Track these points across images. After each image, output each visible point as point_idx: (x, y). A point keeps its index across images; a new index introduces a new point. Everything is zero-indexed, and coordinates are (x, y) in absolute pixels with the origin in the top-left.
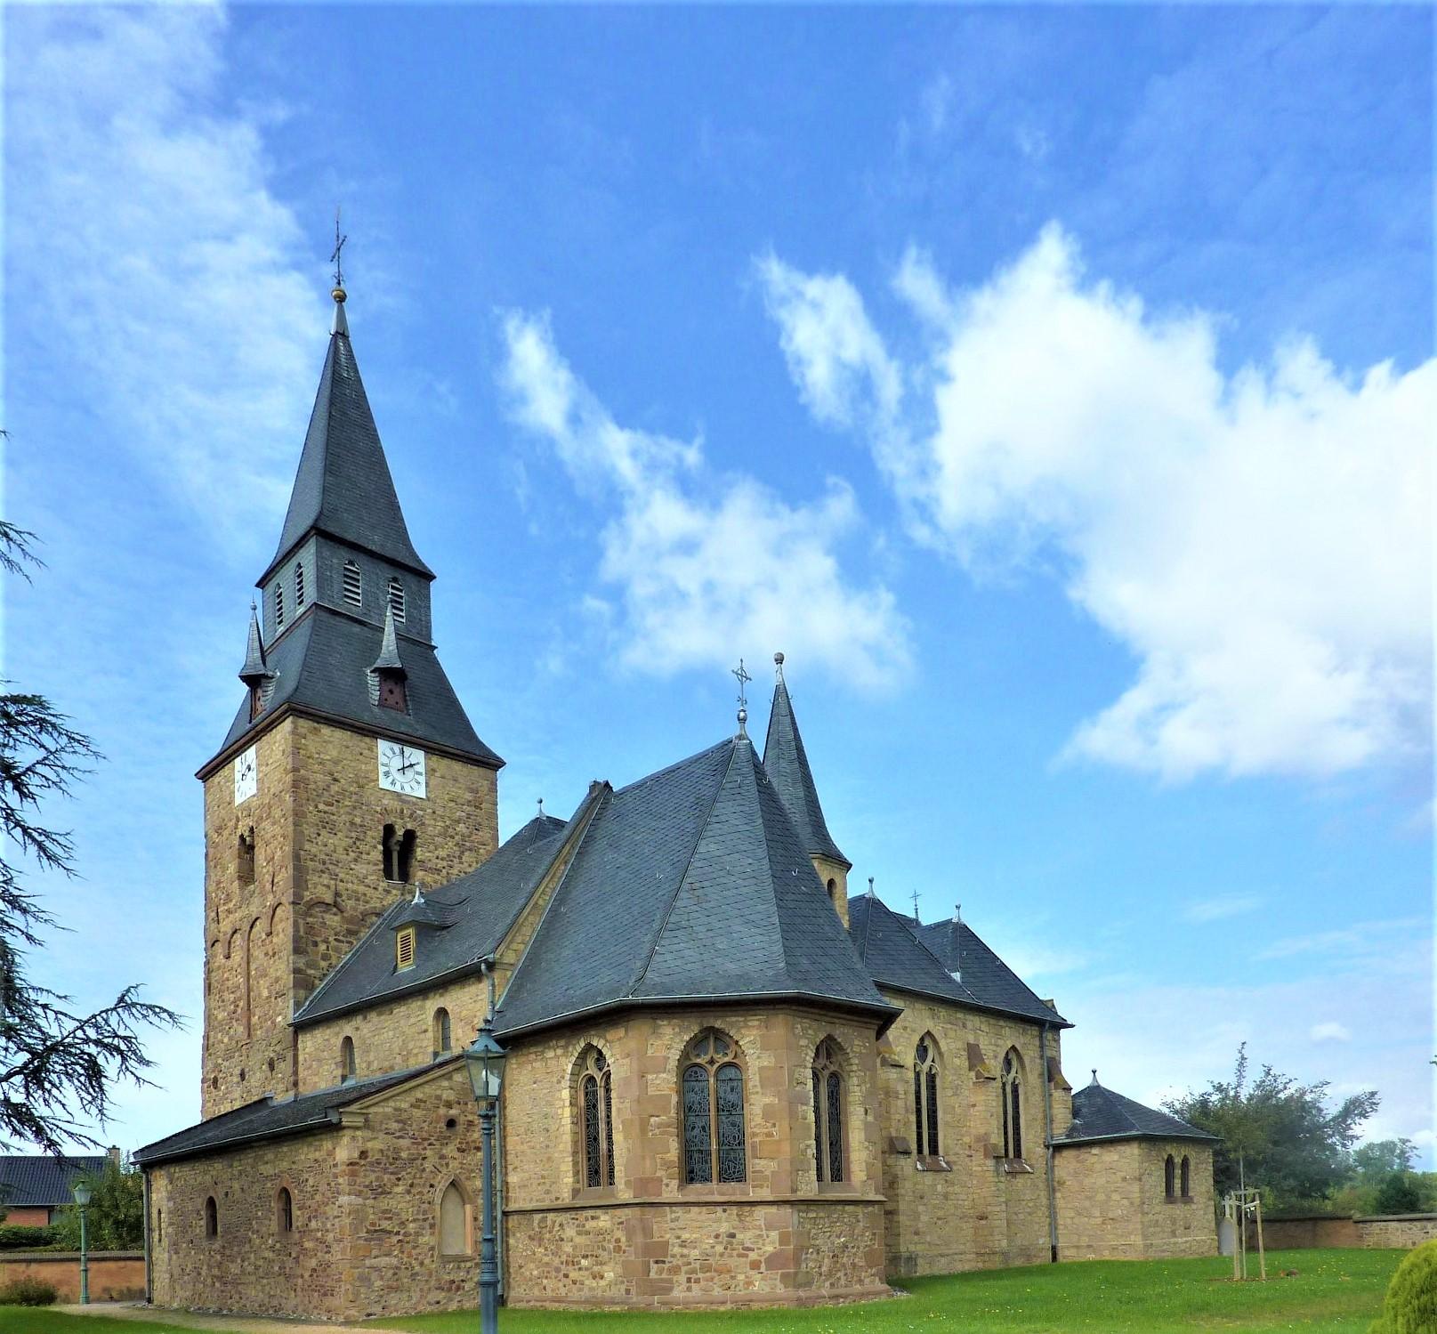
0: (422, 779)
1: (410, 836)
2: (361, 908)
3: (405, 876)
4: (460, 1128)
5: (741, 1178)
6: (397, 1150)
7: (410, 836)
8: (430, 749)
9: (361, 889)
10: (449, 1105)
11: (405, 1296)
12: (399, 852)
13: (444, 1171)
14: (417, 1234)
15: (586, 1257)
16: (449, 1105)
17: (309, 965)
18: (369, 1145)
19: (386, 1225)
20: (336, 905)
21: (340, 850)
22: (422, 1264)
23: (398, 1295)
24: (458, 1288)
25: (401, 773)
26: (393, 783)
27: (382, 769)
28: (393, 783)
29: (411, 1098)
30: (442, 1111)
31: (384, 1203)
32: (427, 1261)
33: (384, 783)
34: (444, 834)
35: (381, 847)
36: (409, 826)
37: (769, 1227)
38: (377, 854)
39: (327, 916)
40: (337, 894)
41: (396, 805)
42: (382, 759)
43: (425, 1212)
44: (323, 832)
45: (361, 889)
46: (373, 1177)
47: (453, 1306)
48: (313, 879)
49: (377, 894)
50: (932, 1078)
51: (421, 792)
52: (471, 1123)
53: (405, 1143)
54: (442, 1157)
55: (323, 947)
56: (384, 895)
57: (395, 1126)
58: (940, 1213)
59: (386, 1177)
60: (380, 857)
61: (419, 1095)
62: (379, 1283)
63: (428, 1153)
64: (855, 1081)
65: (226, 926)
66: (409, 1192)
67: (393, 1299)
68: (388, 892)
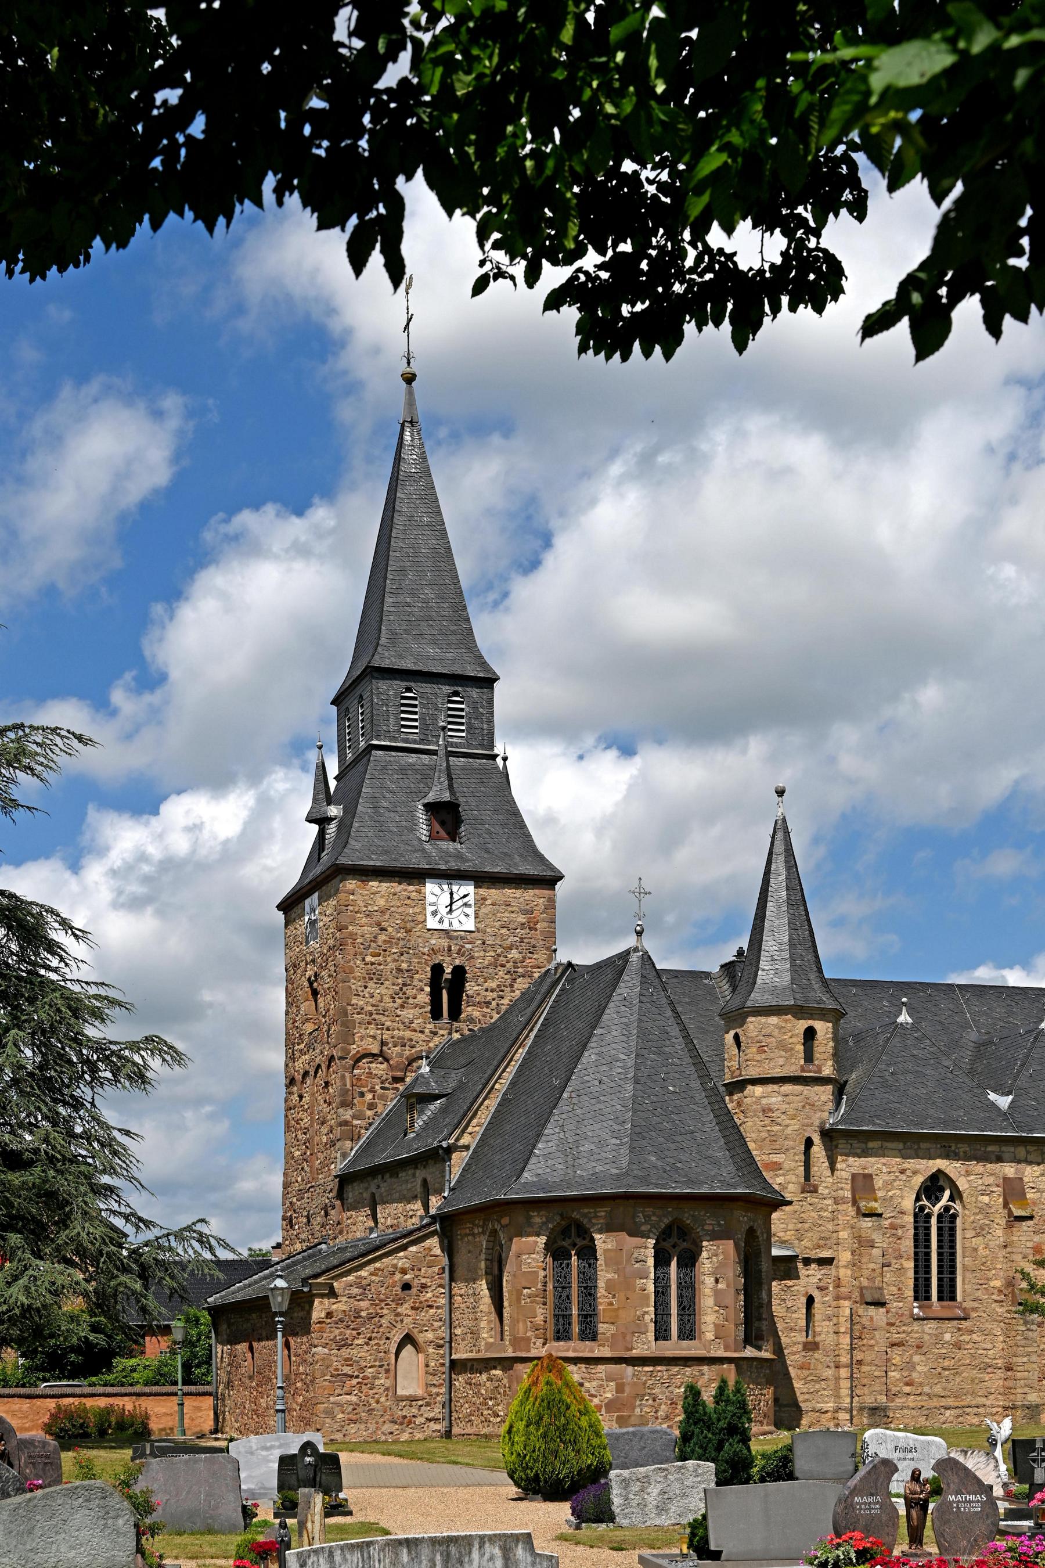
0: (470, 911)
1: (459, 972)
2: (407, 1053)
3: (455, 1013)
4: (414, 1291)
5: (594, 1338)
6: (357, 1311)
7: (459, 972)
8: (480, 879)
9: (408, 1034)
10: (404, 1272)
11: (362, 1427)
12: (448, 989)
13: (399, 1326)
14: (375, 1378)
15: (491, 1399)
16: (404, 1272)
17: (354, 1117)
18: (334, 1307)
19: (347, 1370)
20: (381, 1054)
21: (387, 999)
22: (378, 1402)
23: (358, 1425)
24: (410, 1422)
25: (449, 909)
26: (441, 921)
27: (430, 909)
28: (441, 921)
29: (371, 1268)
30: (398, 1276)
31: (345, 1352)
32: (383, 1399)
33: (432, 923)
34: (494, 965)
35: (428, 989)
36: (457, 962)
37: (609, 1379)
38: (424, 998)
39: (373, 1065)
40: (383, 1043)
41: (444, 943)
42: (431, 899)
43: (381, 1360)
44: (371, 984)
45: (408, 1034)
46: (337, 1332)
47: (405, 1436)
48: (360, 1031)
49: (423, 1037)
50: (948, 1219)
51: (470, 925)
52: (424, 1286)
53: (362, 1303)
54: (398, 1315)
55: (369, 1096)
56: (440, 1036)
57: (355, 1291)
58: (946, 1363)
59: (348, 1332)
60: (427, 999)
61: (377, 1265)
62: (341, 1416)
63: (385, 1311)
64: (704, 1254)
65: (299, 1065)
66: (367, 1344)
67: (352, 1429)
68: (435, 1033)
